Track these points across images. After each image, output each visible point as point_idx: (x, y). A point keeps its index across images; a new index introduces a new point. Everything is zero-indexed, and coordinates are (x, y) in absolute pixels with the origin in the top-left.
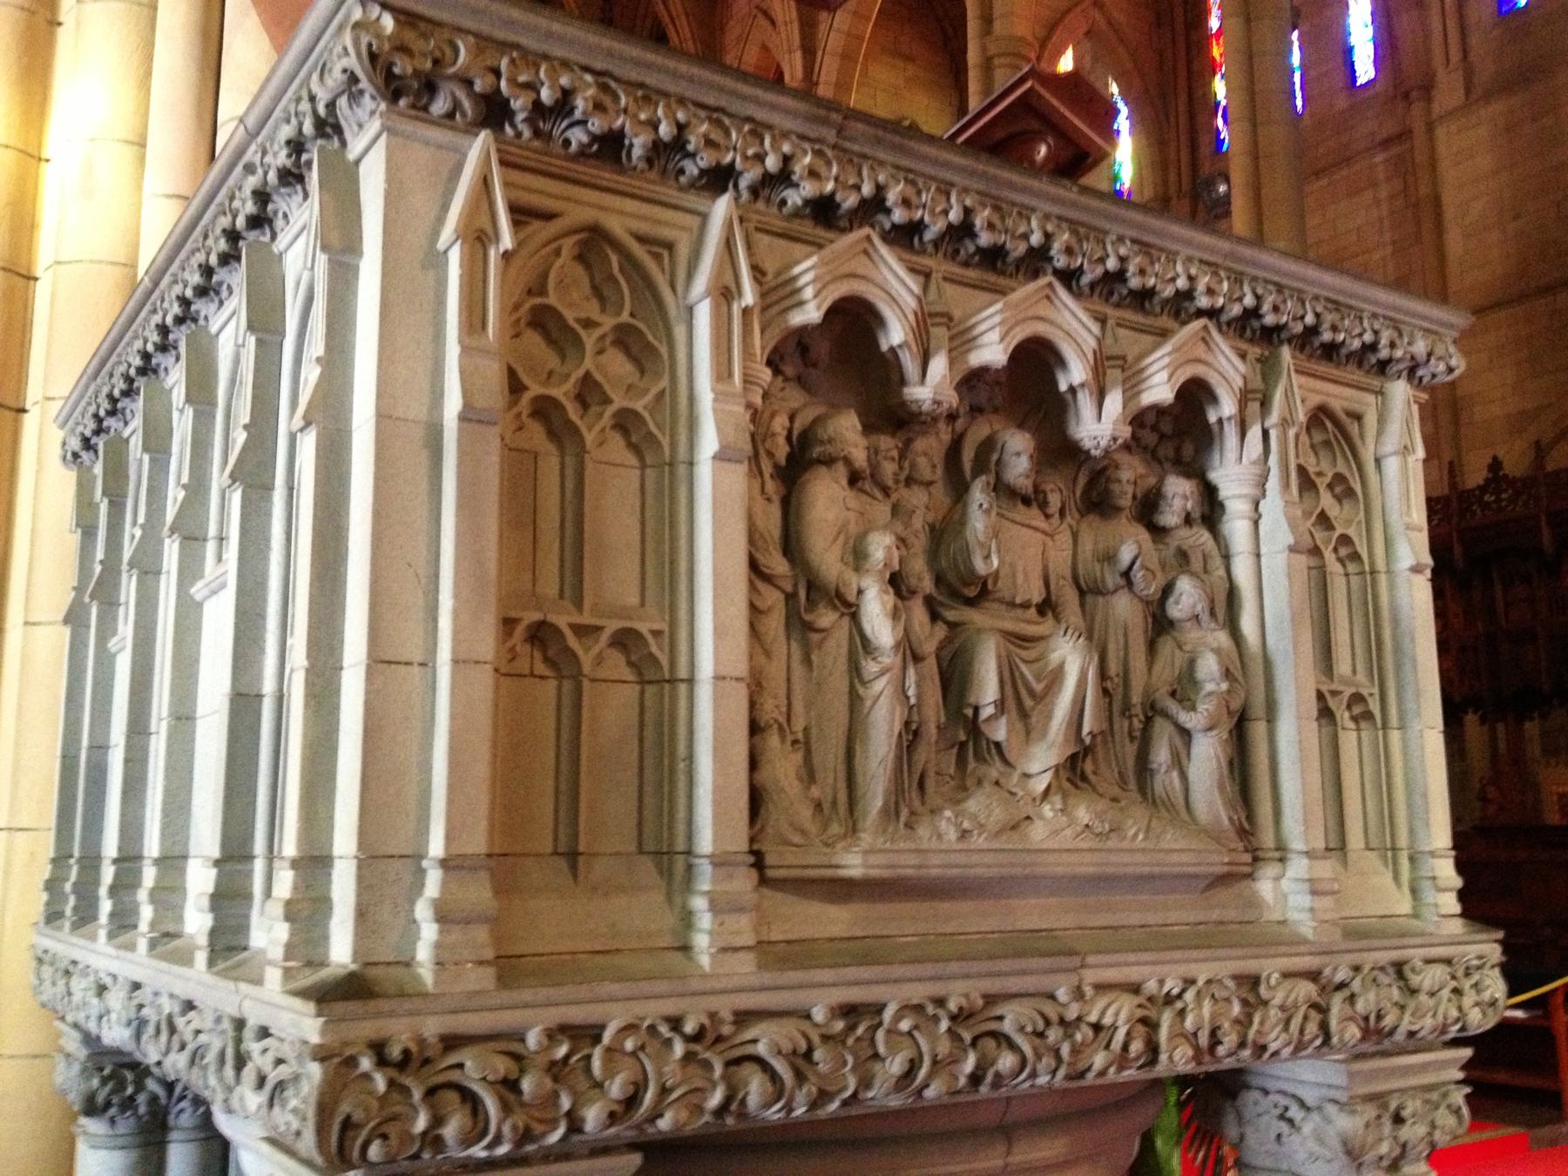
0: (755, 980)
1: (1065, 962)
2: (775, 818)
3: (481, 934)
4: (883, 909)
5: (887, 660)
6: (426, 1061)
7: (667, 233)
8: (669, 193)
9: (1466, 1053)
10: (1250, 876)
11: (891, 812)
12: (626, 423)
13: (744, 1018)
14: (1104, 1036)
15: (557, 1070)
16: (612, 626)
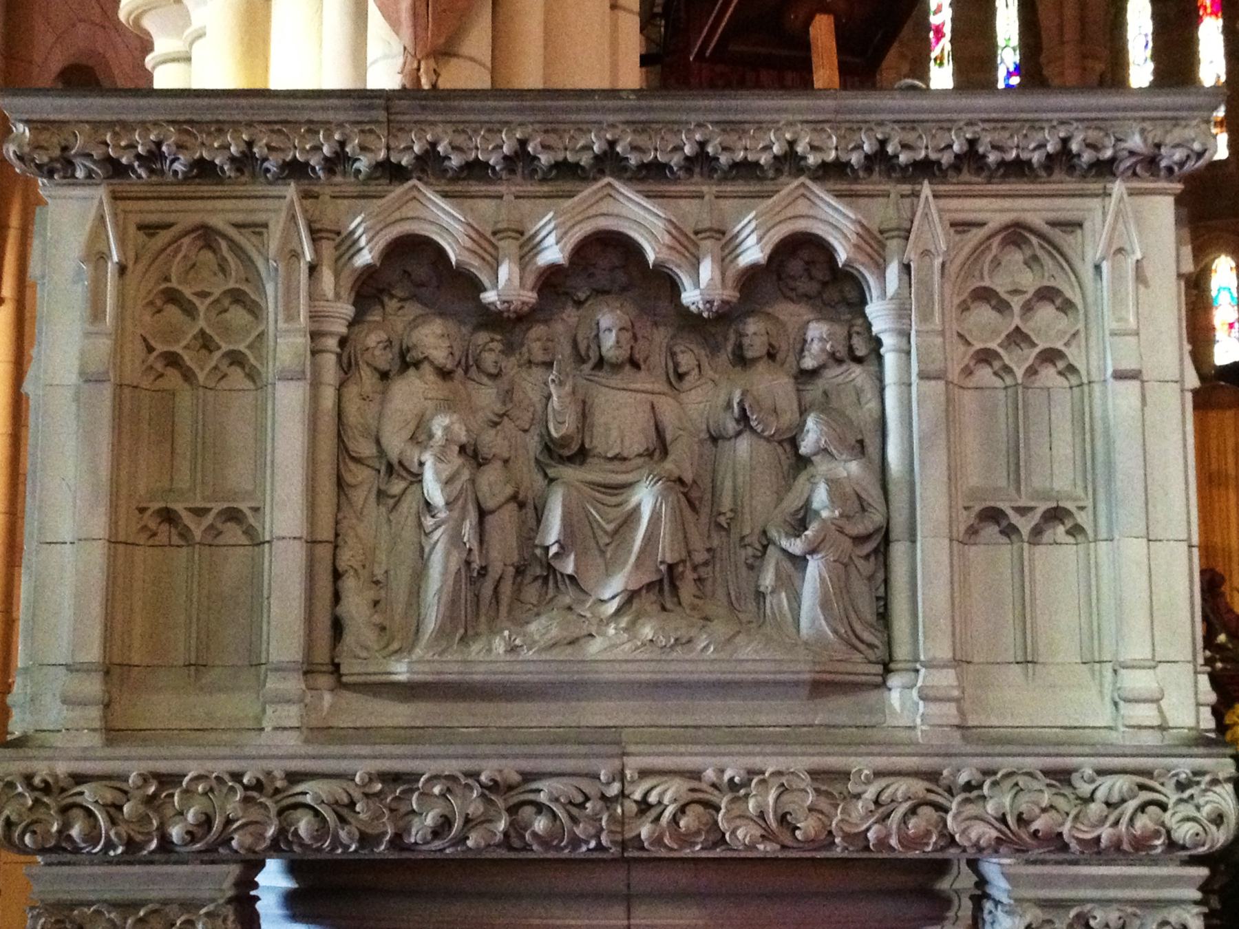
0: (304, 749)
1: (615, 749)
2: (349, 639)
3: (95, 713)
4: (449, 706)
5: (442, 515)
6: (63, 790)
7: (260, 217)
8: (260, 189)
9: (1203, 872)
10: (882, 685)
11: (442, 632)
12: (236, 359)
13: (294, 777)
14: (653, 813)
15: (150, 800)
16: (217, 507)
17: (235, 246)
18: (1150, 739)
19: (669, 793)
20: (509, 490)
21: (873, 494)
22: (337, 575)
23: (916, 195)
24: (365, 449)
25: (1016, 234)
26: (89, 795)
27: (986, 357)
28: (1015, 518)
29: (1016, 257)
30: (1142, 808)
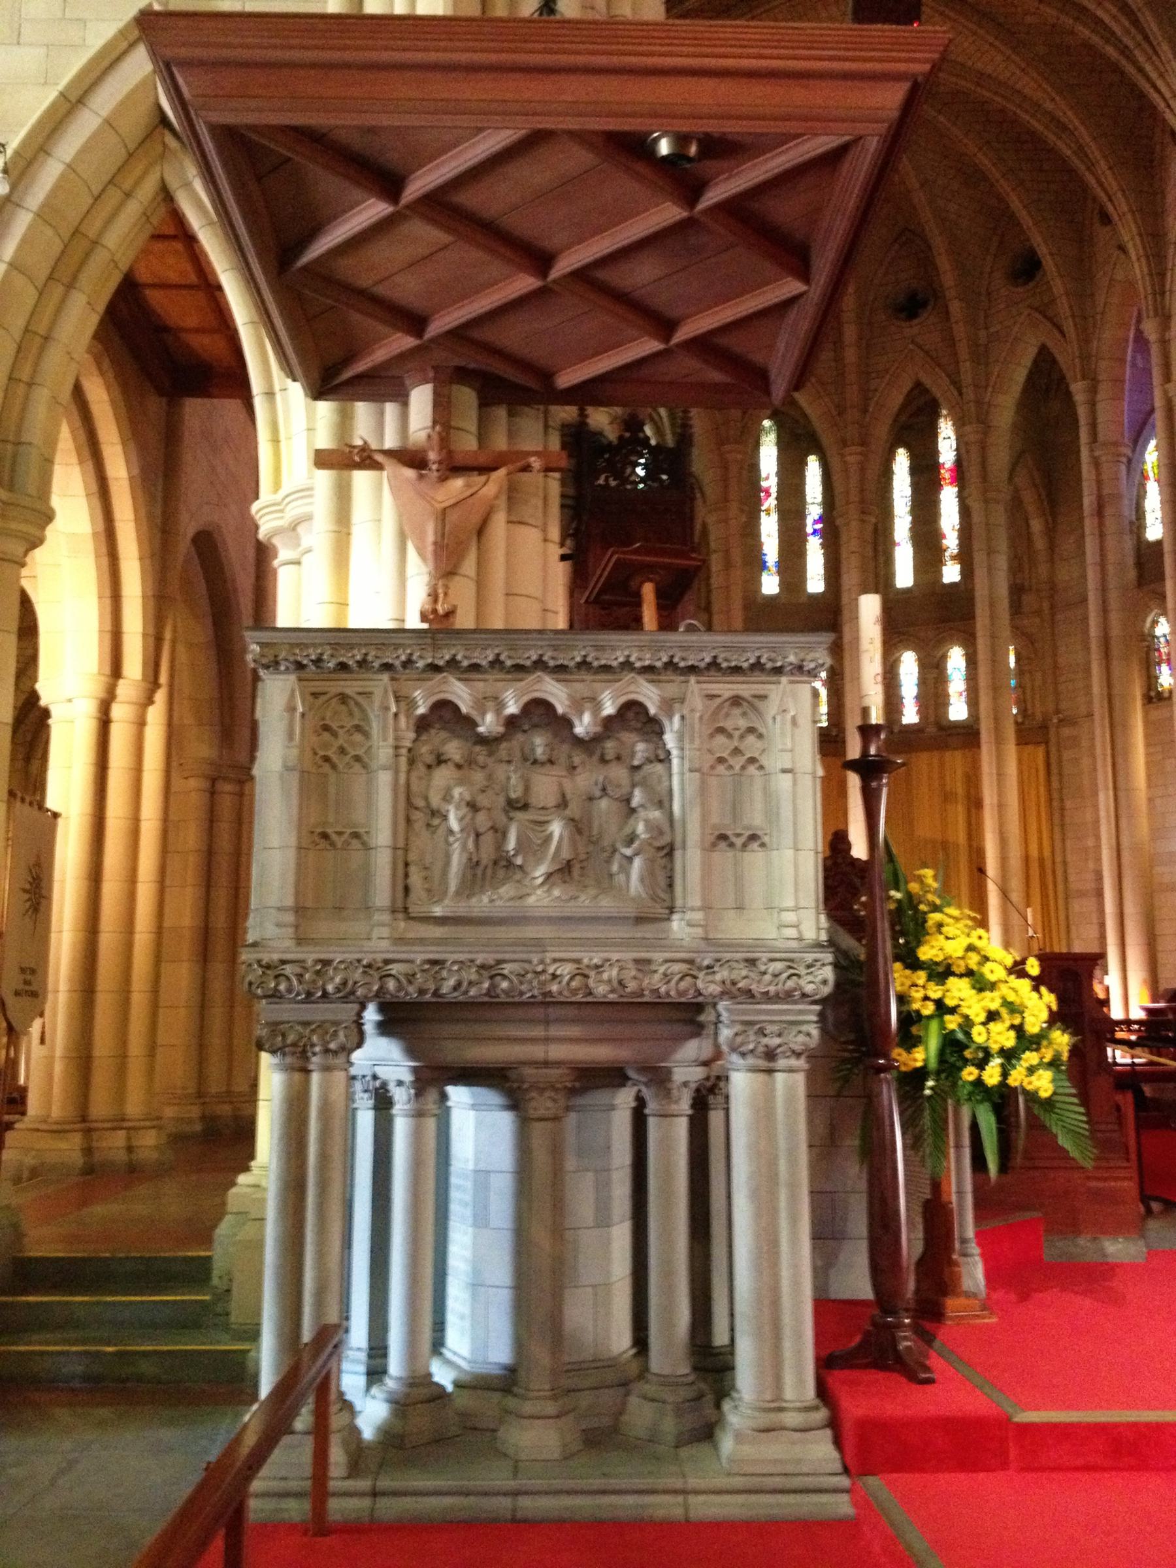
0: (392, 949)
1: (539, 949)
2: (413, 896)
3: (291, 930)
4: (460, 929)
5: (459, 836)
6: (276, 967)
7: (368, 690)
8: (370, 676)
9: (818, 1008)
10: (669, 919)
11: (458, 893)
12: (357, 759)
13: (387, 962)
14: (558, 980)
15: (318, 973)
16: (349, 831)
17: (357, 704)
18: (794, 945)
19: (566, 970)
20: (490, 824)
21: (666, 828)
22: (407, 865)
23: (687, 682)
24: (420, 803)
25: (736, 701)
26: (288, 970)
27: (721, 760)
28: (734, 839)
29: (737, 711)
30: (789, 977)
